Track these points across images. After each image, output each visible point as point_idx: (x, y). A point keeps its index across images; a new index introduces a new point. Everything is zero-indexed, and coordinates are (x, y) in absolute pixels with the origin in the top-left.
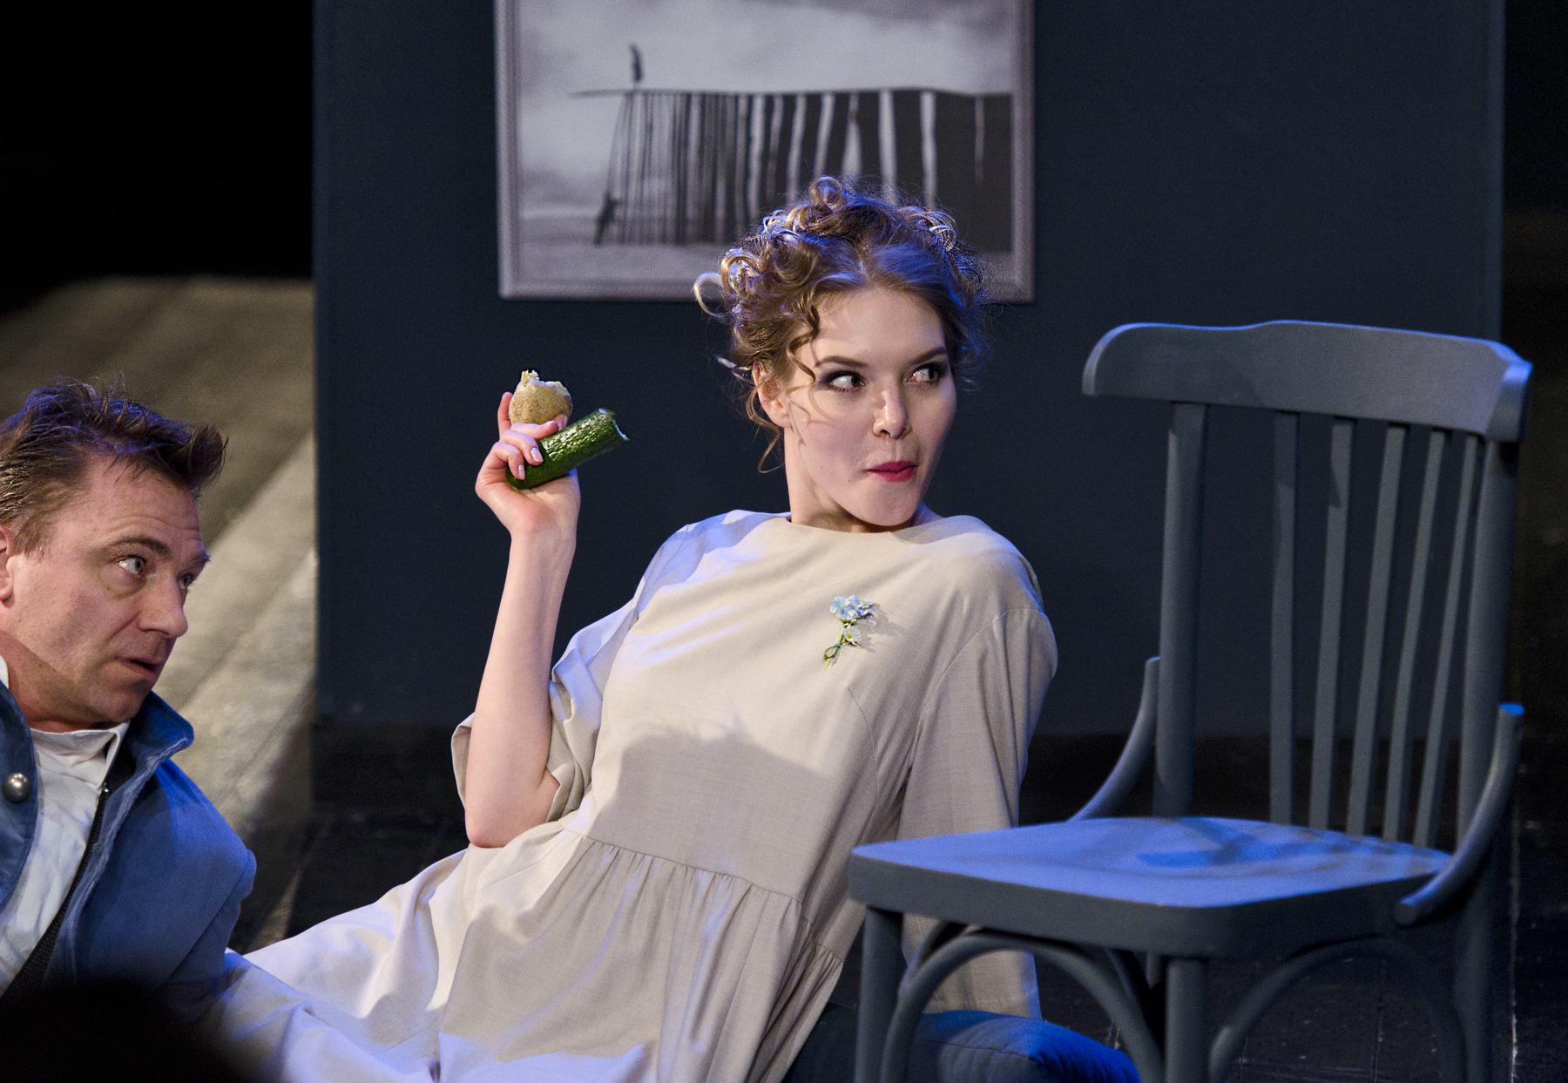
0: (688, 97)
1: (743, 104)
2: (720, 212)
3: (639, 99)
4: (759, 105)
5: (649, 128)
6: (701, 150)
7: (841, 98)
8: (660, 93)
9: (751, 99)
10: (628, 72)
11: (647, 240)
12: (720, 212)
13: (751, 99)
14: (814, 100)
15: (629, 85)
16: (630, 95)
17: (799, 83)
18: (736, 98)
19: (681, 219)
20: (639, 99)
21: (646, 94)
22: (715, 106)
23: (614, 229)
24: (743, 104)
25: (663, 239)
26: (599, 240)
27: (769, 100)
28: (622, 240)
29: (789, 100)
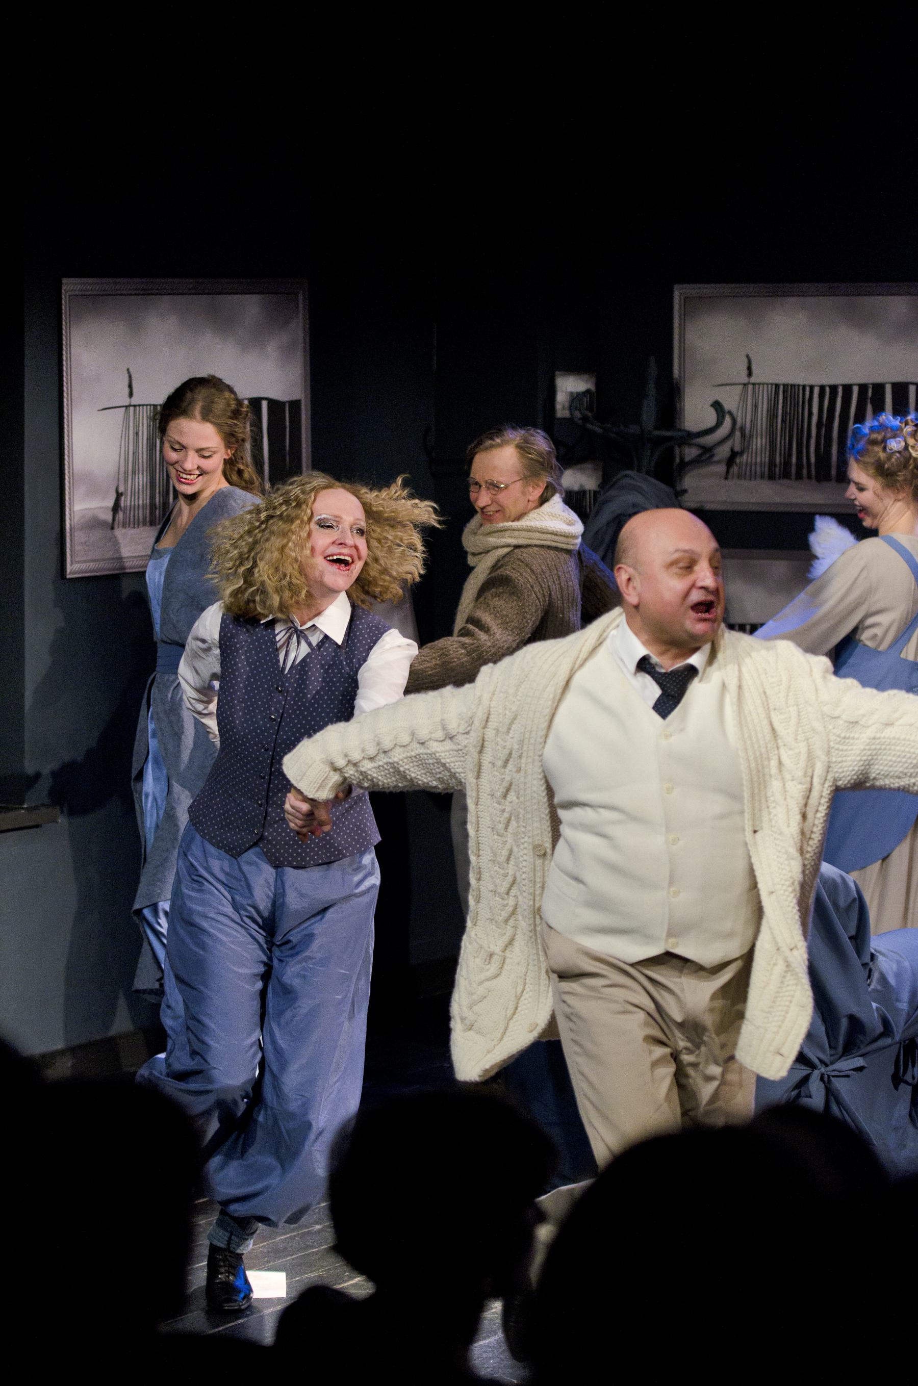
0: (777, 386)
1: (808, 389)
2: (794, 460)
3: (750, 387)
4: (816, 391)
5: (756, 406)
6: (783, 421)
7: (863, 388)
8: (763, 384)
9: (812, 387)
10: (746, 371)
11: (753, 476)
12: (794, 460)
13: (812, 387)
14: (847, 388)
15: (745, 379)
16: (745, 385)
17: (839, 379)
18: (804, 387)
19: (772, 463)
20: (750, 387)
21: (754, 384)
22: (790, 391)
23: (735, 469)
24: (808, 389)
25: (762, 477)
26: (726, 478)
27: (822, 388)
28: (739, 477)
29: (834, 388)
